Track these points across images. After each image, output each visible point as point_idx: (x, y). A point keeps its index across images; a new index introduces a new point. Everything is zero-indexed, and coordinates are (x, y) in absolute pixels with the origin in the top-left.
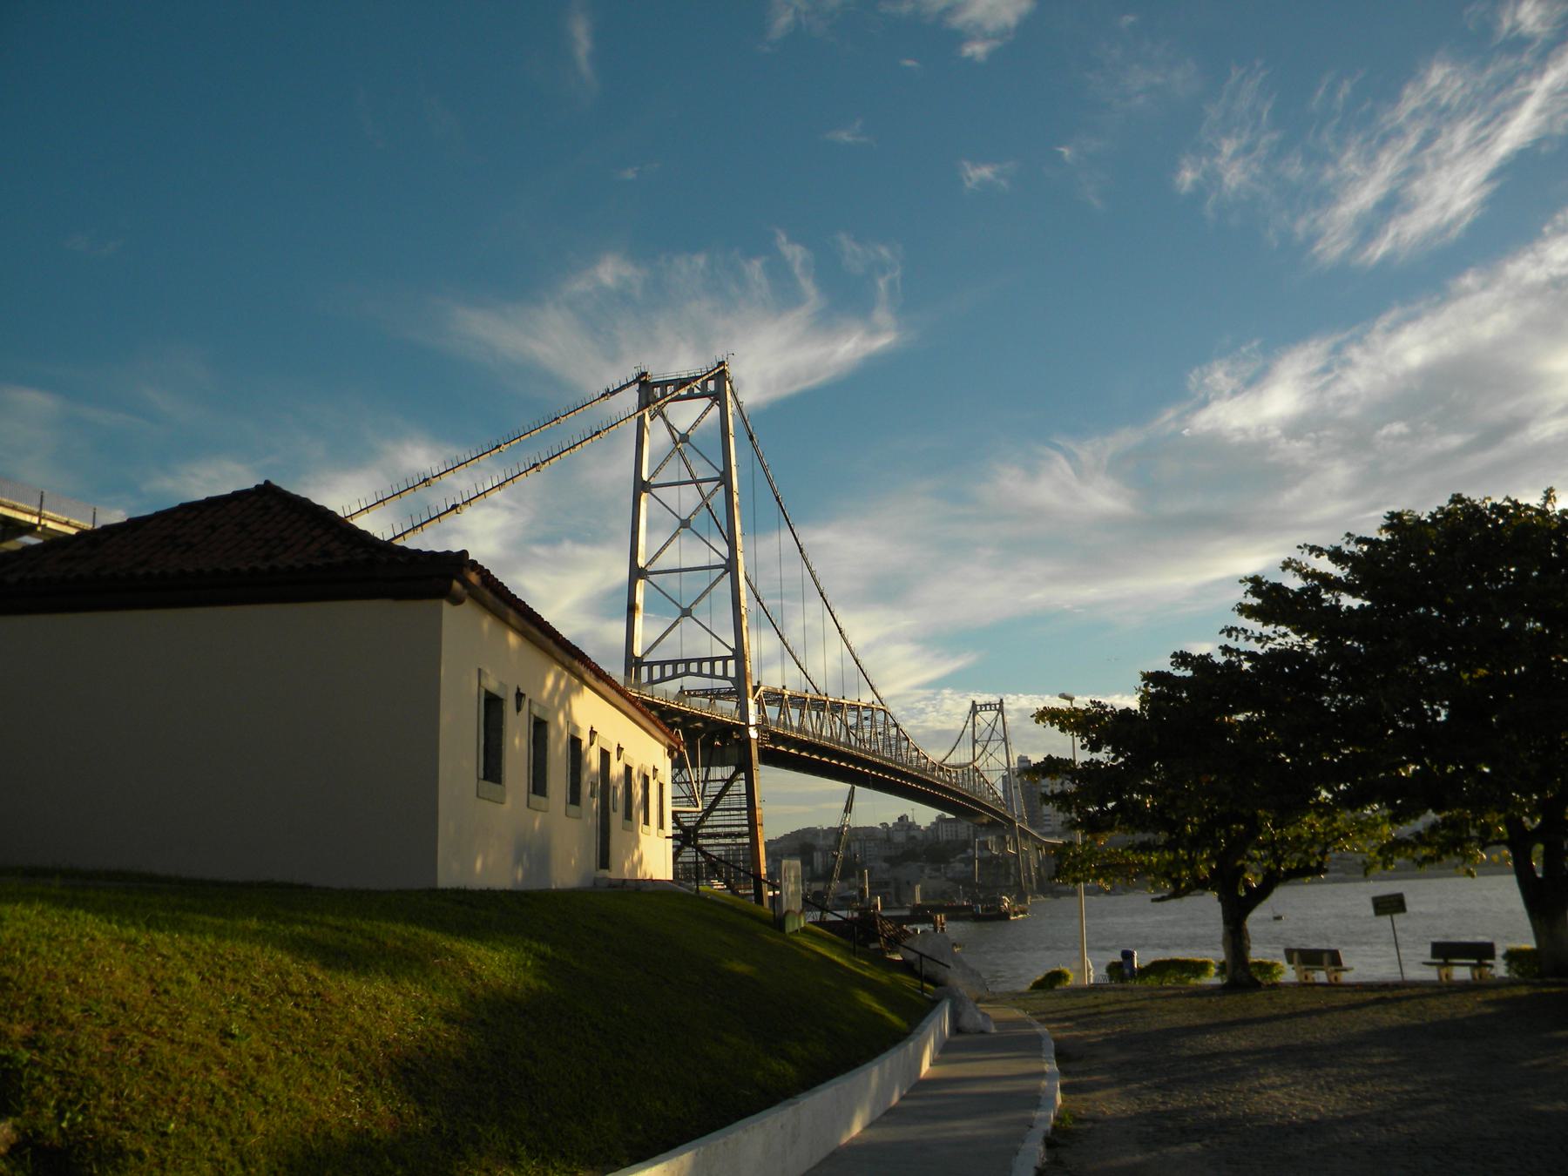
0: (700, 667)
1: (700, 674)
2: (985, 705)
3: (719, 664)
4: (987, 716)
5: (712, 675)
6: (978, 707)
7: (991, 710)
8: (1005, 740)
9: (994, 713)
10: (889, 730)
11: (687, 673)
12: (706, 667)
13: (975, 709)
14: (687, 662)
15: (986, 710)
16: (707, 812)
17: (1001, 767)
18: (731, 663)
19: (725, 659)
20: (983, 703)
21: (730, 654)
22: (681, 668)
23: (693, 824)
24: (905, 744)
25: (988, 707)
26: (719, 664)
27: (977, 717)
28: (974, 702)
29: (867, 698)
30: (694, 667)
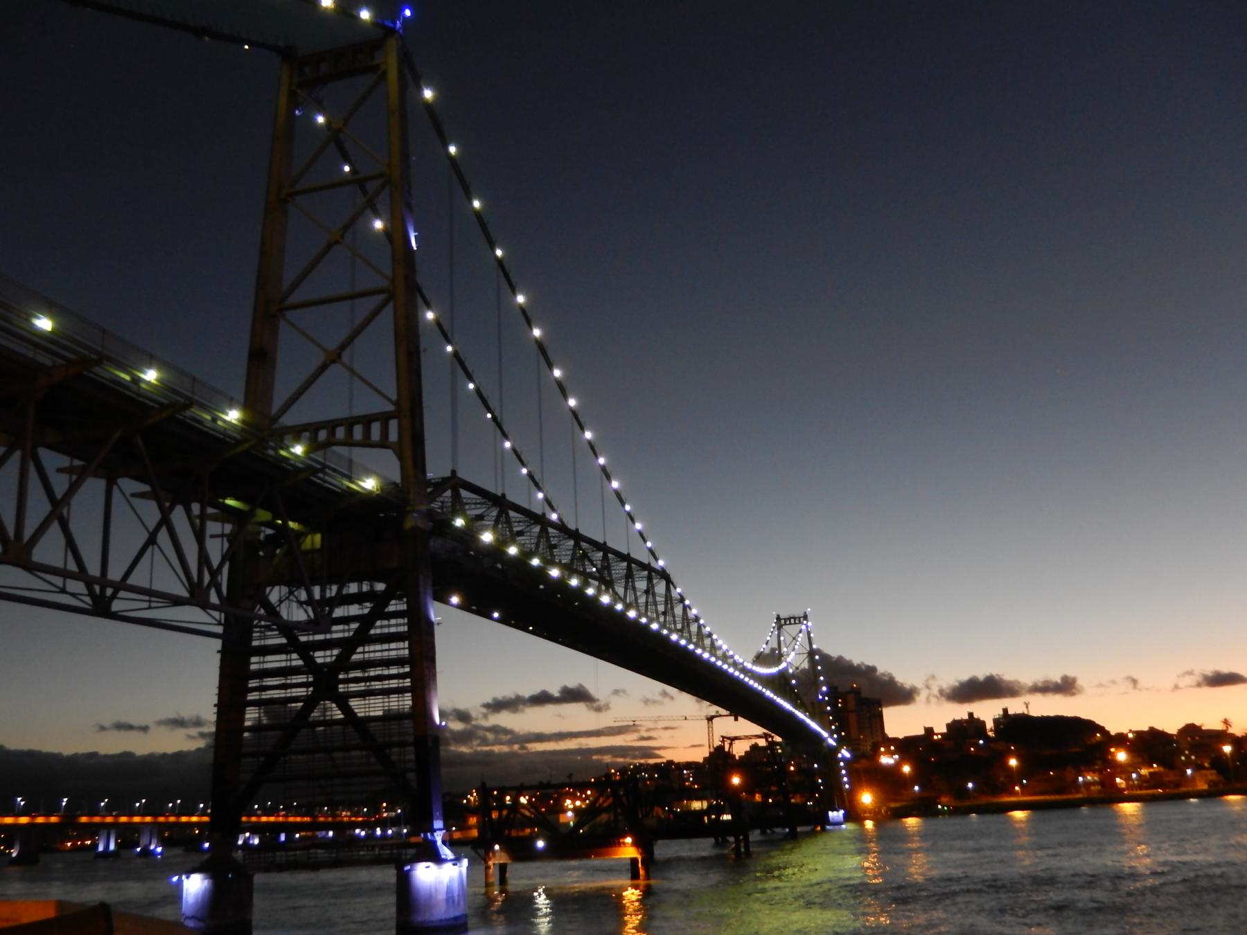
0: (350, 432)
1: (349, 442)
2: (790, 619)
3: (376, 429)
5: (366, 443)
6: (783, 622)
7: (795, 623)
10: (672, 608)
12: (358, 432)
14: (332, 425)
15: (790, 624)
16: (348, 646)
18: (393, 425)
19: (384, 418)
21: (391, 408)
22: (323, 435)
23: (328, 660)
25: (792, 621)
26: (376, 429)
27: (782, 630)
30: (340, 433)
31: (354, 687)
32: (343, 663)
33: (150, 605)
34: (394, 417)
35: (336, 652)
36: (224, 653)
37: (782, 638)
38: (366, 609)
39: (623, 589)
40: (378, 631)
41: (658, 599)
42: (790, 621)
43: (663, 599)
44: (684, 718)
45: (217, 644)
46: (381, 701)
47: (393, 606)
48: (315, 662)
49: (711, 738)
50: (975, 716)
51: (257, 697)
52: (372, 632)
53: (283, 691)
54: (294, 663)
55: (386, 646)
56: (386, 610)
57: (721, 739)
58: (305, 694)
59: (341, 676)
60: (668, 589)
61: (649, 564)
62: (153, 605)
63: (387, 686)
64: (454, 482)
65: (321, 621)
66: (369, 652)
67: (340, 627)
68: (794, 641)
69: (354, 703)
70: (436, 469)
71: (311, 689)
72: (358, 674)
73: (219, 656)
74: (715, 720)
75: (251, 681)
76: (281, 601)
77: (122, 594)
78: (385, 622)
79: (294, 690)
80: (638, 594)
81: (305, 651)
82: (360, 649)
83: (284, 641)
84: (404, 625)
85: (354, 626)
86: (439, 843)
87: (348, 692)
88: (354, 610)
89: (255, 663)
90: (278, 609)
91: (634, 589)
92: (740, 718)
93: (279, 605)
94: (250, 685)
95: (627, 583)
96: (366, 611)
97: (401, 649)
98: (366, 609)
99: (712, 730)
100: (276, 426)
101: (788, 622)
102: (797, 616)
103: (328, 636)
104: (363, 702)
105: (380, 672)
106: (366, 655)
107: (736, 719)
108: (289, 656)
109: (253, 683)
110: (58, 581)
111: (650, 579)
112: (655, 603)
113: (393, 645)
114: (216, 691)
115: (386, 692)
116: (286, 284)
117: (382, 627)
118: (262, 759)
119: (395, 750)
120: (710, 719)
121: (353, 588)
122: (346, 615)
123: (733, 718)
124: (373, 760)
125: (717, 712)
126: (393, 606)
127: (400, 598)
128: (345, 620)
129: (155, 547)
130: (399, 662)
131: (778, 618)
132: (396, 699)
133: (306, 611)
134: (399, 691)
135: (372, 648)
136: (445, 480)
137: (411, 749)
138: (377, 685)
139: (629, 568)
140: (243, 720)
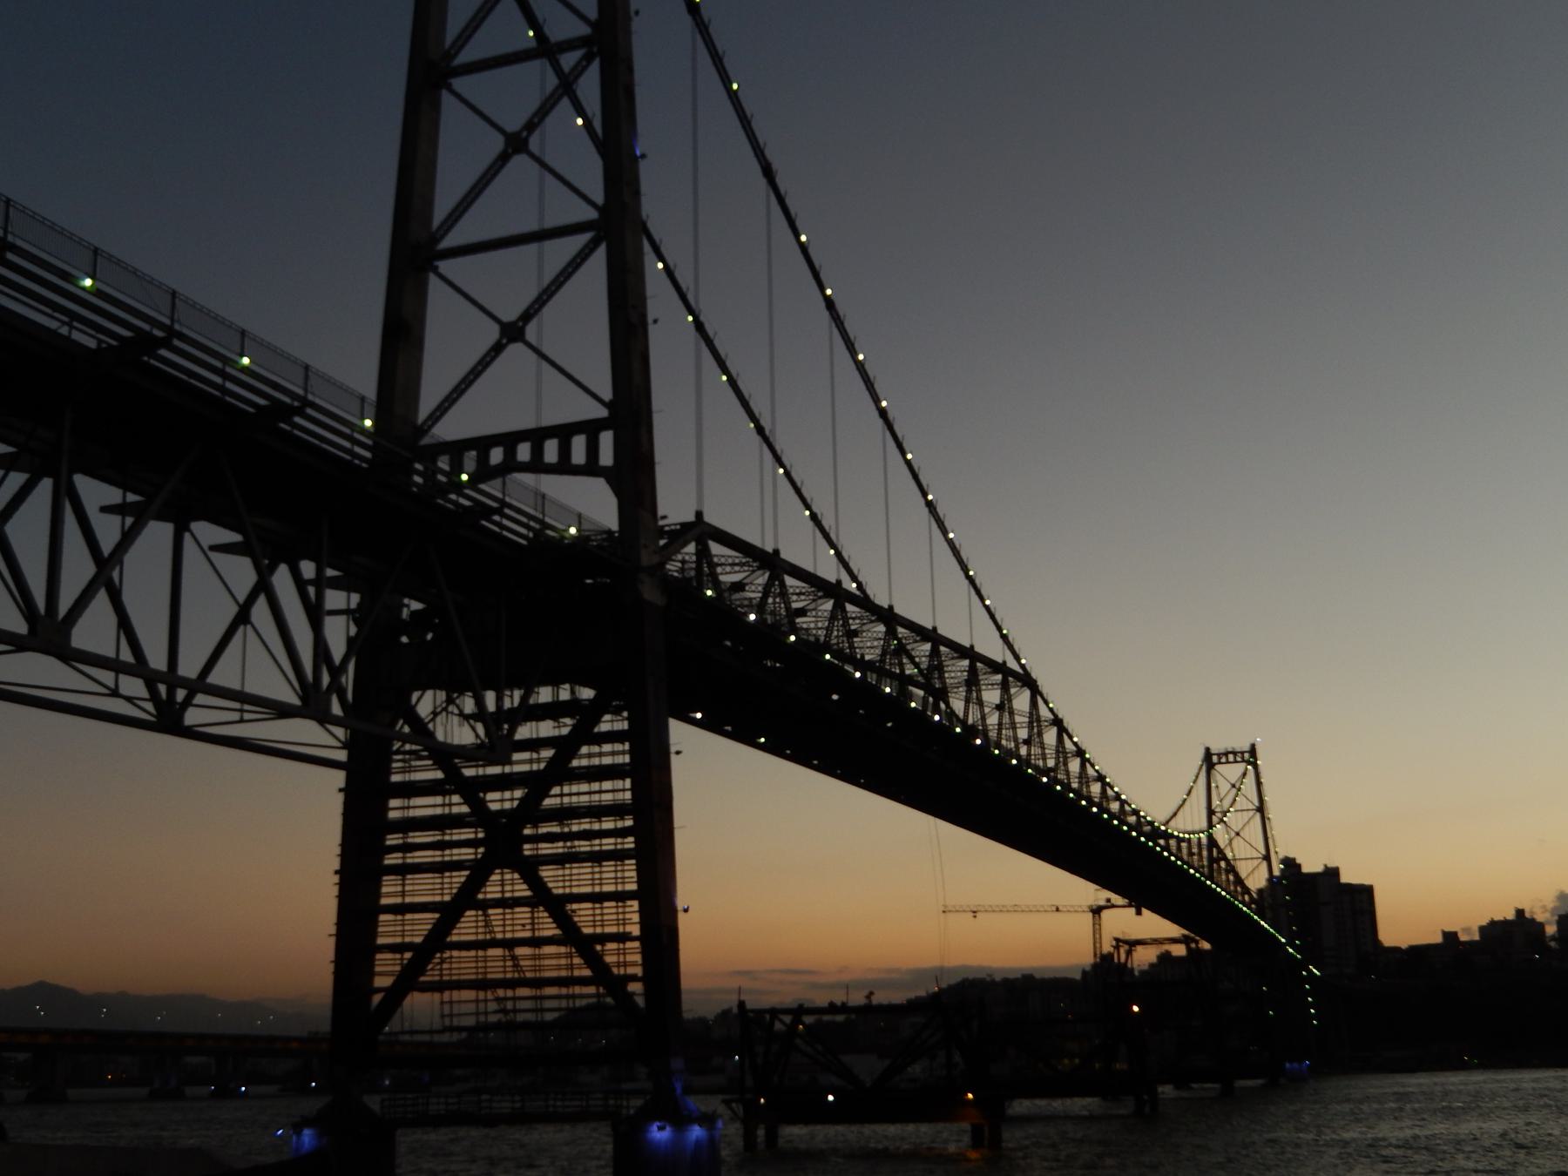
0: (538, 451)
1: (537, 465)
2: (1226, 754)
3: (579, 445)
4: (1228, 772)
5: (564, 467)
6: (1215, 759)
7: (1236, 762)
8: (1261, 809)
9: (1241, 767)
11: (510, 466)
13: (1210, 761)
14: (509, 440)
15: (1228, 762)
16: (538, 784)
17: (1256, 854)
18: (606, 439)
19: (591, 429)
20: (1222, 751)
21: (603, 413)
22: (496, 456)
23: (507, 805)
24: (1074, 765)
25: (1231, 757)
26: (579, 445)
27: (1213, 772)
28: (1208, 750)
29: (992, 648)
30: (524, 452)
31: (546, 849)
32: (530, 811)
33: (242, 717)
34: (606, 428)
35: (518, 793)
36: (349, 791)
37: (1213, 785)
38: (565, 726)
39: (963, 703)
40: (584, 762)
41: (1018, 719)
42: (1227, 759)
43: (1027, 720)
44: (1054, 909)
45: (339, 778)
46: (589, 870)
47: (606, 725)
48: (487, 809)
49: (1098, 940)
50: (1527, 915)
51: (400, 861)
52: (575, 763)
53: (439, 853)
54: (455, 810)
55: (595, 786)
56: (596, 730)
57: (1114, 943)
58: (472, 857)
59: (527, 832)
60: (1034, 704)
61: (1005, 663)
62: (247, 716)
63: (597, 848)
64: (700, 531)
65: (498, 746)
66: (570, 795)
67: (526, 755)
68: (1234, 791)
69: (547, 873)
70: (674, 507)
71: (481, 850)
72: (554, 828)
73: (340, 797)
74: (1105, 914)
75: (389, 837)
76: (435, 714)
77: (200, 698)
78: (596, 749)
79: (455, 851)
80: (987, 710)
81: (473, 790)
82: (556, 790)
83: (439, 775)
84: (623, 753)
85: (547, 753)
86: (679, 1091)
87: (537, 856)
88: (546, 729)
89: (396, 809)
90: (431, 726)
91: (980, 703)
92: (1144, 911)
93: (433, 720)
94: (388, 843)
95: (969, 691)
96: (565, 731)
97: (620, 791)
98: (565, 726)
99: (1100, 929)
100: (426, 441)
101: (1223, 760)
102: (1239, 750)
103: (507, 769)
104: (560, 872)
105: (587, 827)
106: (566, 800)
107: (1139, 913)
108: (447, 798)
109: (393, 840)
110: (107, 677)
111: (1005, 687)
112: (1013, 726)
113: (607, 785)
114: (338, 850)
115: (598, 858)
116: (439, 217)
117: (590, 756)
118: (408, 955)
119: (611, 946)
120: (1097, 911)
121: (544, 695)
122: (534, 736)
123: (1133, 910)
124: (577, 961)
125: (1108, 900)
126: (606, 725)
127: (617, 712)
128: (534, 745)
129: (249, 627)
130: (616, 810)
131: (1208, 754)
132: (613, 869)
133: (474, 729)
134: (618, 856)
135: (575, 788)
136: (686, 527)
137: (637, 944)
138: (583, 846)
139: (972, 671)
140: (378, 895)
